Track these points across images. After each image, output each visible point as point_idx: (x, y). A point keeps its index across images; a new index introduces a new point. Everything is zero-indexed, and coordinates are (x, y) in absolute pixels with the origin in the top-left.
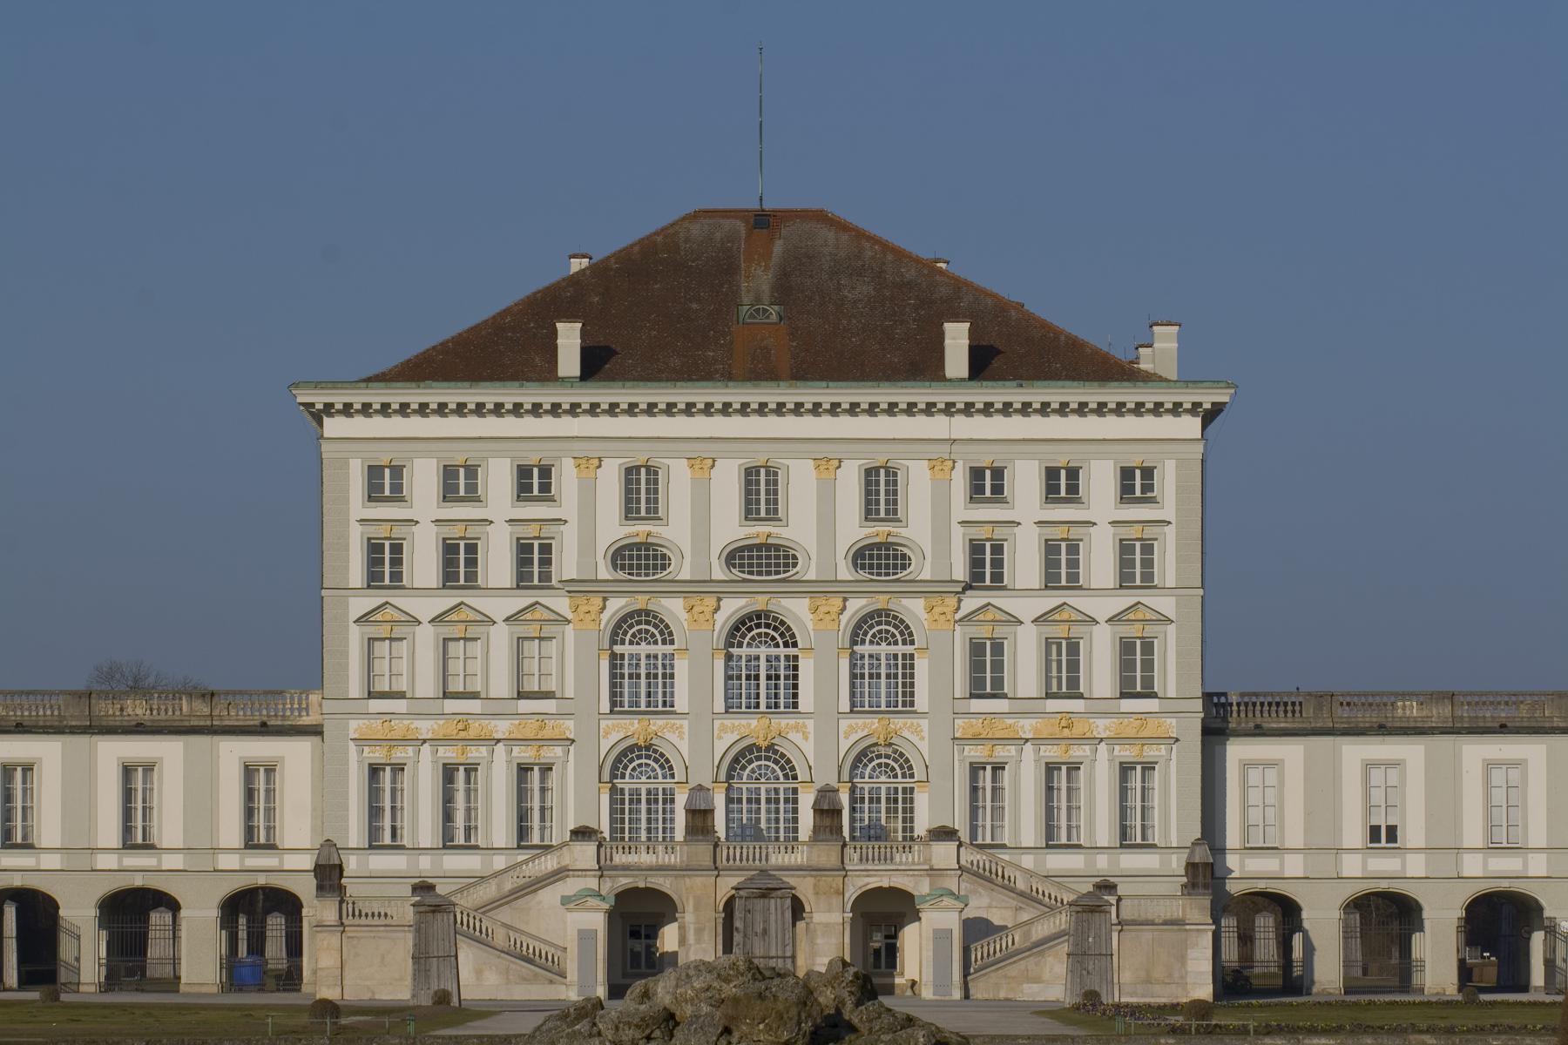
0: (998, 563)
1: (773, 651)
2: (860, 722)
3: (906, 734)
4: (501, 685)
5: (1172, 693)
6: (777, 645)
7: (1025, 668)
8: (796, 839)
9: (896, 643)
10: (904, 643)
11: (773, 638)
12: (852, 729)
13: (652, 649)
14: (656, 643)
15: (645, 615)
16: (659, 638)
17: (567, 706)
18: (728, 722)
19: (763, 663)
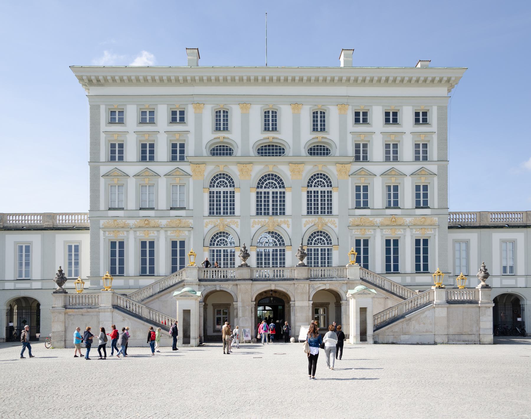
0: (365, 152)
1: (275, 190)
2: (311, 219)
3: (329, 224)
4: (163, 204)
5: (436, 206)
6: (276, 187)
7: (378, 197)
8: (284, 267)
9: (324, 186)
10: (328, 186)
11: (275, 184)
12: (307, 222)
13: (226, 189)
14: (227, 186)
15: (223, 175)
16: (228, 184)
17: (190, 213)
18: (256, 220)
19: (271, 195)
